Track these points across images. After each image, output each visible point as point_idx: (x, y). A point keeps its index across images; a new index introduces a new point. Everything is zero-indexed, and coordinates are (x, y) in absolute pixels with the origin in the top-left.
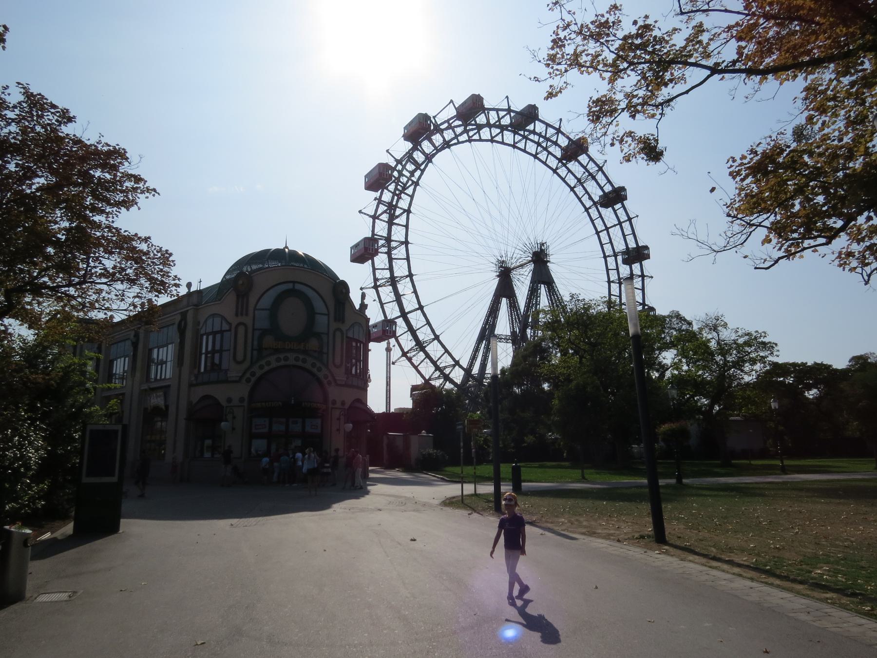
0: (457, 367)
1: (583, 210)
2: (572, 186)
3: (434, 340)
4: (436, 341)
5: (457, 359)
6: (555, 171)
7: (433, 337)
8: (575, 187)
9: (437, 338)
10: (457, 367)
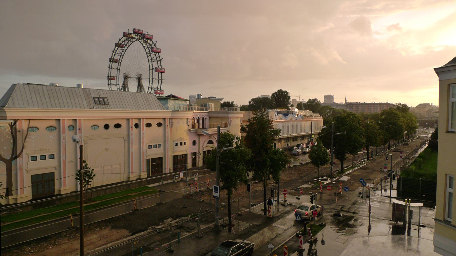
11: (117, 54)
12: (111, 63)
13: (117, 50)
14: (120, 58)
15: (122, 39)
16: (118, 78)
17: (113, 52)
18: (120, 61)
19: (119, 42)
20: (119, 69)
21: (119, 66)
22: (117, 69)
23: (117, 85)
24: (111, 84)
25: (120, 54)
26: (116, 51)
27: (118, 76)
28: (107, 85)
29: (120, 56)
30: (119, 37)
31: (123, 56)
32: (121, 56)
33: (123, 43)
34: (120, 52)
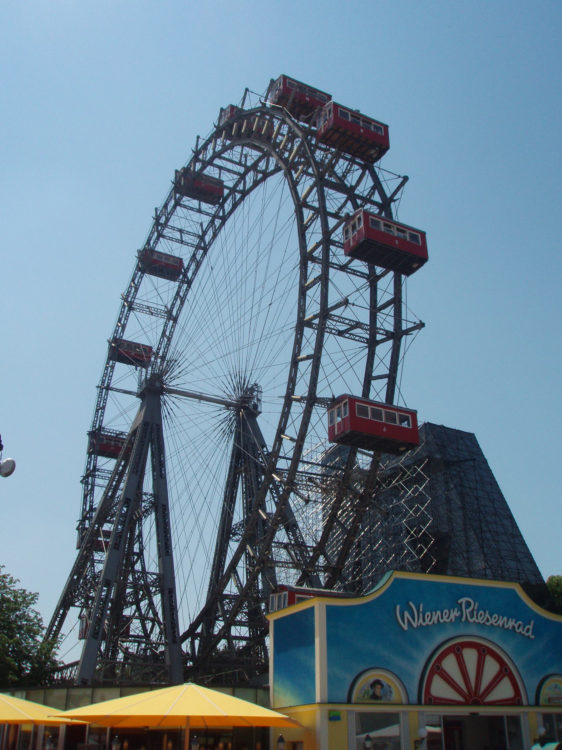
13: (175, 207)
15: (205, 147)
17: (157, 218)
18: (190, 275)
20: (174, 313)
24: (108, 388)
30: (198, 137)
31: (205, 250)
34: (201, 224)
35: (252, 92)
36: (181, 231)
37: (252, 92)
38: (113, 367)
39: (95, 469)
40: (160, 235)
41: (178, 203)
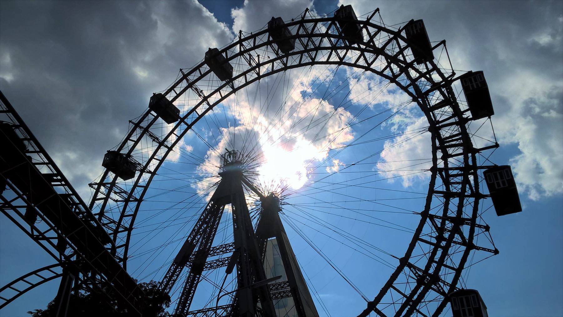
0: (431, 212)
1: (171, 152)
2: (150, 175)
3: (410, 266)
4: (411, 261)
5: (420, 217)
6: (140, 201)
7: (406, 269)
8: (149, 172)
9: (404, 262)
10: (431, 212)
11: (248, 57)
12: (206, 68)
14: (244, 74)
16: (183, 126)
19: (293, 23)
21: (217, 97)
22: (205, 99)
23: (161, 144)
24: (146, 131)
25: (254, 64)
26: (255, 47)
27: (189, 121)
28: (130, 121)
29: (247, 67)
31: (259, 77)
32: (253, 69)
33: (305, 40)
35: (379, 13)
36: (250, 55)
37: (379, 13)
38: (156, 118)
39: (113, 184)
40: (241, 53)
41: (268, 43)
